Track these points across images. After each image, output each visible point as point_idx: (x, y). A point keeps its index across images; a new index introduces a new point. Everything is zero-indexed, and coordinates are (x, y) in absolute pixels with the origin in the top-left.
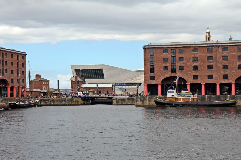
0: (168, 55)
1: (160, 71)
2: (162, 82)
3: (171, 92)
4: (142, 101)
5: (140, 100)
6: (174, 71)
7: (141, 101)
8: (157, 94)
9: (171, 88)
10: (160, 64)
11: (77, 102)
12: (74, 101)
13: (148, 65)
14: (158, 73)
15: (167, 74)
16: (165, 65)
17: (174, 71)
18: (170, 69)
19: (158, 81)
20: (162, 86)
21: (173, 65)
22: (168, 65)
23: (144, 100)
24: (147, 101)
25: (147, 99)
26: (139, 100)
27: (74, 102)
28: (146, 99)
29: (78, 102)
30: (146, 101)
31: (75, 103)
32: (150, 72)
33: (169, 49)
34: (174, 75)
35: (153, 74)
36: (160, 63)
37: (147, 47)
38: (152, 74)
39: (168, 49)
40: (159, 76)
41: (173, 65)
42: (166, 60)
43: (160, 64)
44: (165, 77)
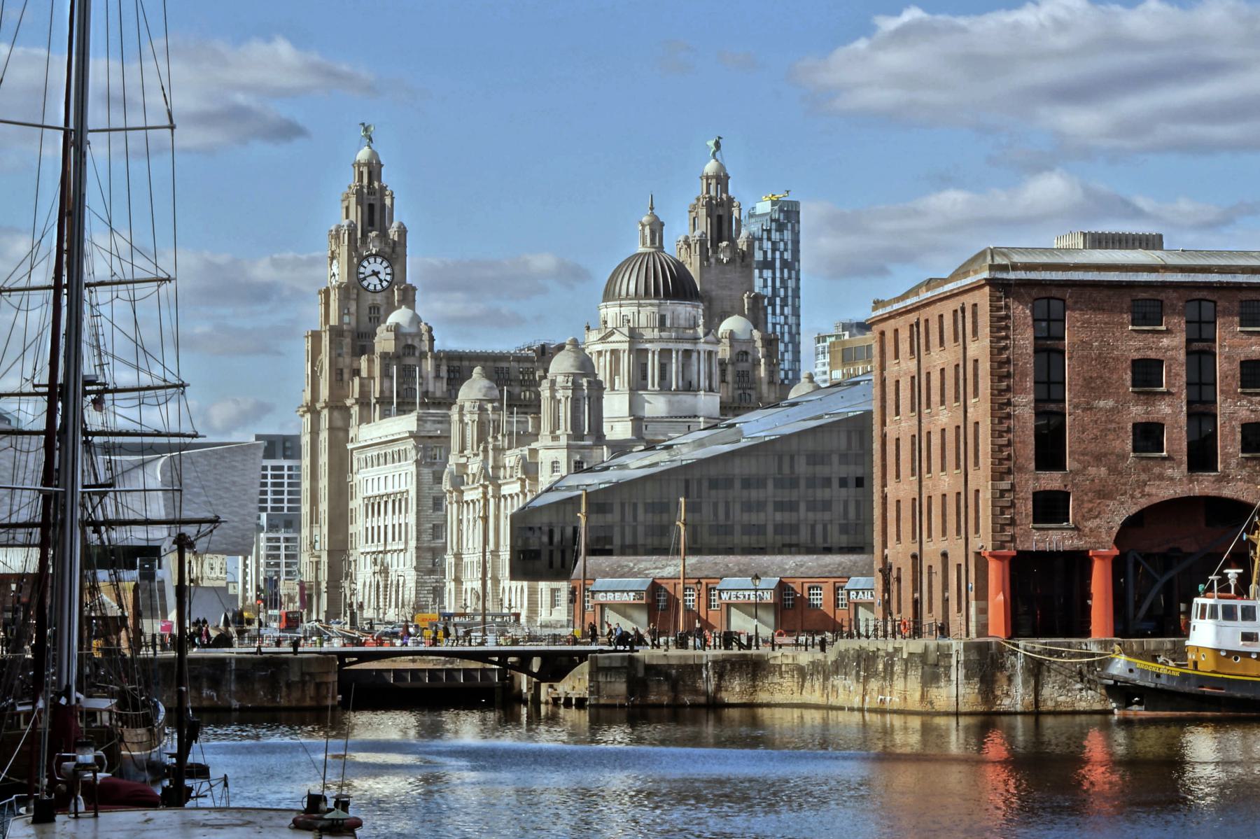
0: (1165, 341)
1: (1105, 455)
2: (1118, 541)
3: (1229, 614)
4: (982, 681)
5: (962, 672)
6: (1202, 455)
7: (967, 677)
8: (1086, 633)
9: (1224, 587)
10: (1111, 403)
11: (311, 691)
12: (295, 678)
13: (1024, 405)
14: (1092, 471)
15: (1161, 477)
16: (1137, 412)
17: (1202, 455)
18: (1176, 439)
19: (1096, 530)
20: (1118, 567)
21: (1201, 413)
22: (1171, 411)
23: (994, 675)
24: (1019, 680)
25: (1020, 663)
26: (958, 673)
27: (289, 685)
28: (1008, 664)
29: (318, 686)
30: (1010, 679)
31: (296, 694)
32: (1033, 465)
33: (1173, 295)
34: (1204, 486)
35: (1057, 475)
36: (1107, 396)
37: (1012, 276)
38: (1052, 481)
39: (1162, 296)
40: (1104, 494)
41: (1201, 413)
42: (1147, 374)
43: (1111, 403)
44: (1144, 503)
